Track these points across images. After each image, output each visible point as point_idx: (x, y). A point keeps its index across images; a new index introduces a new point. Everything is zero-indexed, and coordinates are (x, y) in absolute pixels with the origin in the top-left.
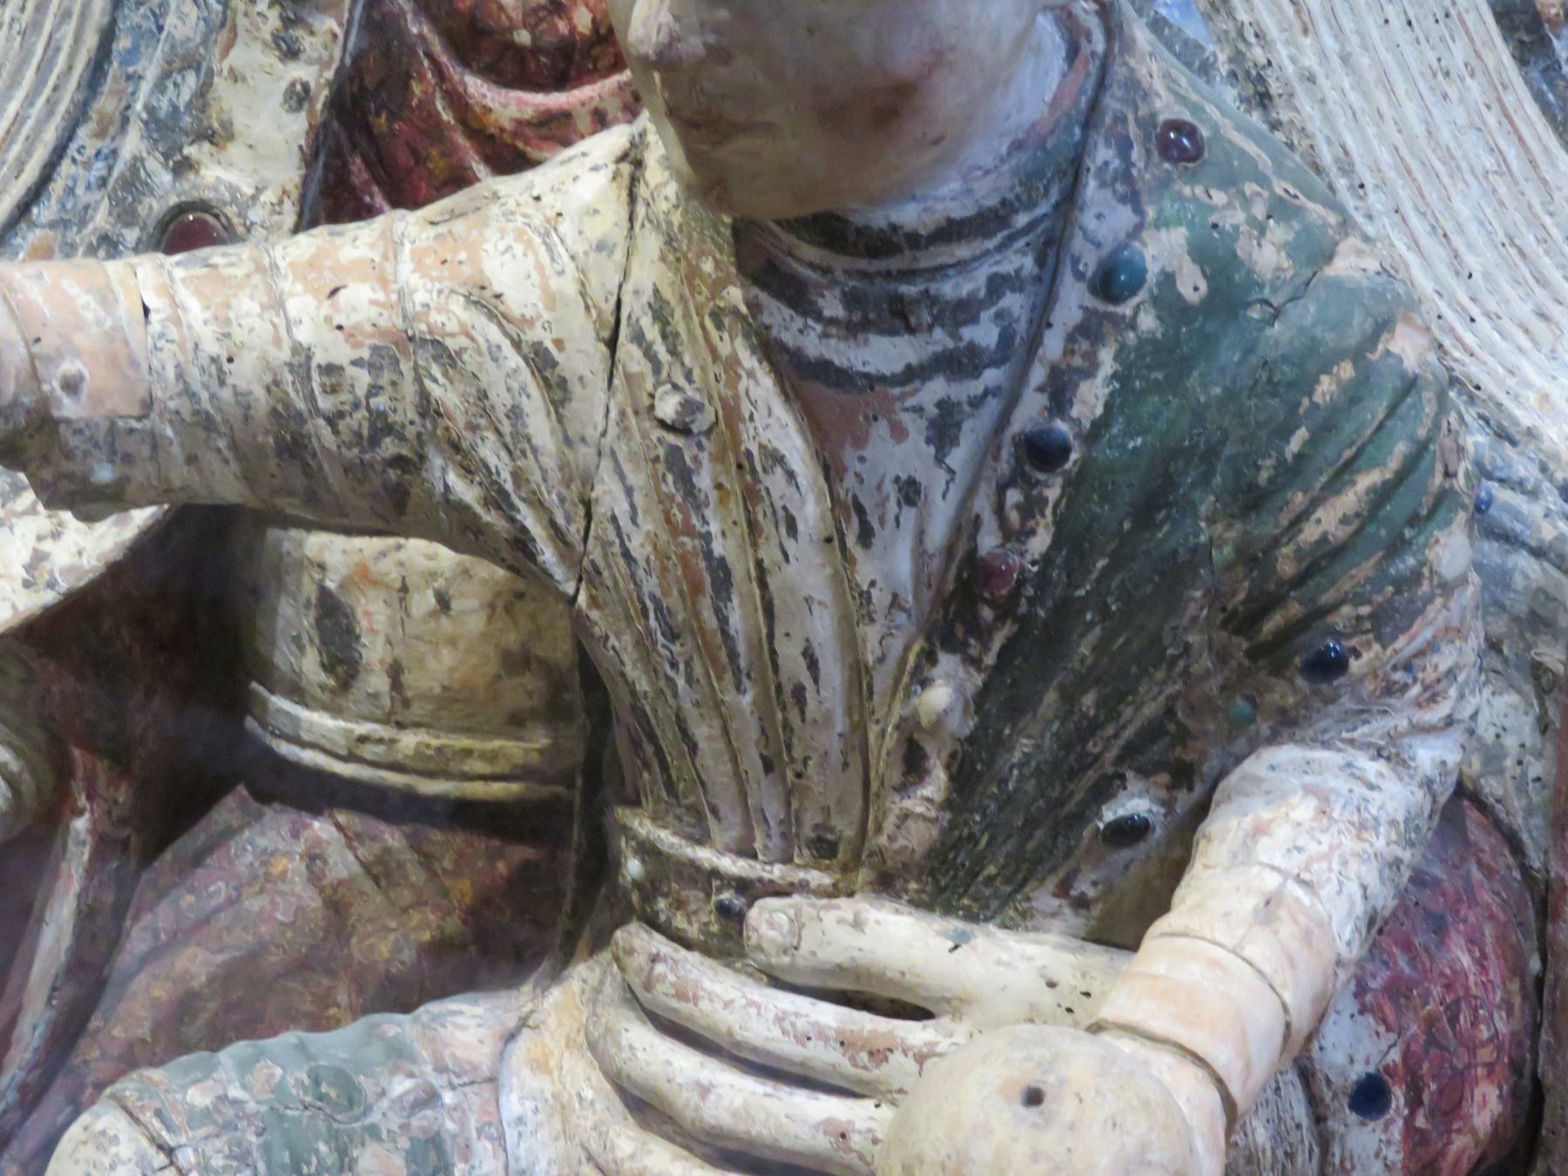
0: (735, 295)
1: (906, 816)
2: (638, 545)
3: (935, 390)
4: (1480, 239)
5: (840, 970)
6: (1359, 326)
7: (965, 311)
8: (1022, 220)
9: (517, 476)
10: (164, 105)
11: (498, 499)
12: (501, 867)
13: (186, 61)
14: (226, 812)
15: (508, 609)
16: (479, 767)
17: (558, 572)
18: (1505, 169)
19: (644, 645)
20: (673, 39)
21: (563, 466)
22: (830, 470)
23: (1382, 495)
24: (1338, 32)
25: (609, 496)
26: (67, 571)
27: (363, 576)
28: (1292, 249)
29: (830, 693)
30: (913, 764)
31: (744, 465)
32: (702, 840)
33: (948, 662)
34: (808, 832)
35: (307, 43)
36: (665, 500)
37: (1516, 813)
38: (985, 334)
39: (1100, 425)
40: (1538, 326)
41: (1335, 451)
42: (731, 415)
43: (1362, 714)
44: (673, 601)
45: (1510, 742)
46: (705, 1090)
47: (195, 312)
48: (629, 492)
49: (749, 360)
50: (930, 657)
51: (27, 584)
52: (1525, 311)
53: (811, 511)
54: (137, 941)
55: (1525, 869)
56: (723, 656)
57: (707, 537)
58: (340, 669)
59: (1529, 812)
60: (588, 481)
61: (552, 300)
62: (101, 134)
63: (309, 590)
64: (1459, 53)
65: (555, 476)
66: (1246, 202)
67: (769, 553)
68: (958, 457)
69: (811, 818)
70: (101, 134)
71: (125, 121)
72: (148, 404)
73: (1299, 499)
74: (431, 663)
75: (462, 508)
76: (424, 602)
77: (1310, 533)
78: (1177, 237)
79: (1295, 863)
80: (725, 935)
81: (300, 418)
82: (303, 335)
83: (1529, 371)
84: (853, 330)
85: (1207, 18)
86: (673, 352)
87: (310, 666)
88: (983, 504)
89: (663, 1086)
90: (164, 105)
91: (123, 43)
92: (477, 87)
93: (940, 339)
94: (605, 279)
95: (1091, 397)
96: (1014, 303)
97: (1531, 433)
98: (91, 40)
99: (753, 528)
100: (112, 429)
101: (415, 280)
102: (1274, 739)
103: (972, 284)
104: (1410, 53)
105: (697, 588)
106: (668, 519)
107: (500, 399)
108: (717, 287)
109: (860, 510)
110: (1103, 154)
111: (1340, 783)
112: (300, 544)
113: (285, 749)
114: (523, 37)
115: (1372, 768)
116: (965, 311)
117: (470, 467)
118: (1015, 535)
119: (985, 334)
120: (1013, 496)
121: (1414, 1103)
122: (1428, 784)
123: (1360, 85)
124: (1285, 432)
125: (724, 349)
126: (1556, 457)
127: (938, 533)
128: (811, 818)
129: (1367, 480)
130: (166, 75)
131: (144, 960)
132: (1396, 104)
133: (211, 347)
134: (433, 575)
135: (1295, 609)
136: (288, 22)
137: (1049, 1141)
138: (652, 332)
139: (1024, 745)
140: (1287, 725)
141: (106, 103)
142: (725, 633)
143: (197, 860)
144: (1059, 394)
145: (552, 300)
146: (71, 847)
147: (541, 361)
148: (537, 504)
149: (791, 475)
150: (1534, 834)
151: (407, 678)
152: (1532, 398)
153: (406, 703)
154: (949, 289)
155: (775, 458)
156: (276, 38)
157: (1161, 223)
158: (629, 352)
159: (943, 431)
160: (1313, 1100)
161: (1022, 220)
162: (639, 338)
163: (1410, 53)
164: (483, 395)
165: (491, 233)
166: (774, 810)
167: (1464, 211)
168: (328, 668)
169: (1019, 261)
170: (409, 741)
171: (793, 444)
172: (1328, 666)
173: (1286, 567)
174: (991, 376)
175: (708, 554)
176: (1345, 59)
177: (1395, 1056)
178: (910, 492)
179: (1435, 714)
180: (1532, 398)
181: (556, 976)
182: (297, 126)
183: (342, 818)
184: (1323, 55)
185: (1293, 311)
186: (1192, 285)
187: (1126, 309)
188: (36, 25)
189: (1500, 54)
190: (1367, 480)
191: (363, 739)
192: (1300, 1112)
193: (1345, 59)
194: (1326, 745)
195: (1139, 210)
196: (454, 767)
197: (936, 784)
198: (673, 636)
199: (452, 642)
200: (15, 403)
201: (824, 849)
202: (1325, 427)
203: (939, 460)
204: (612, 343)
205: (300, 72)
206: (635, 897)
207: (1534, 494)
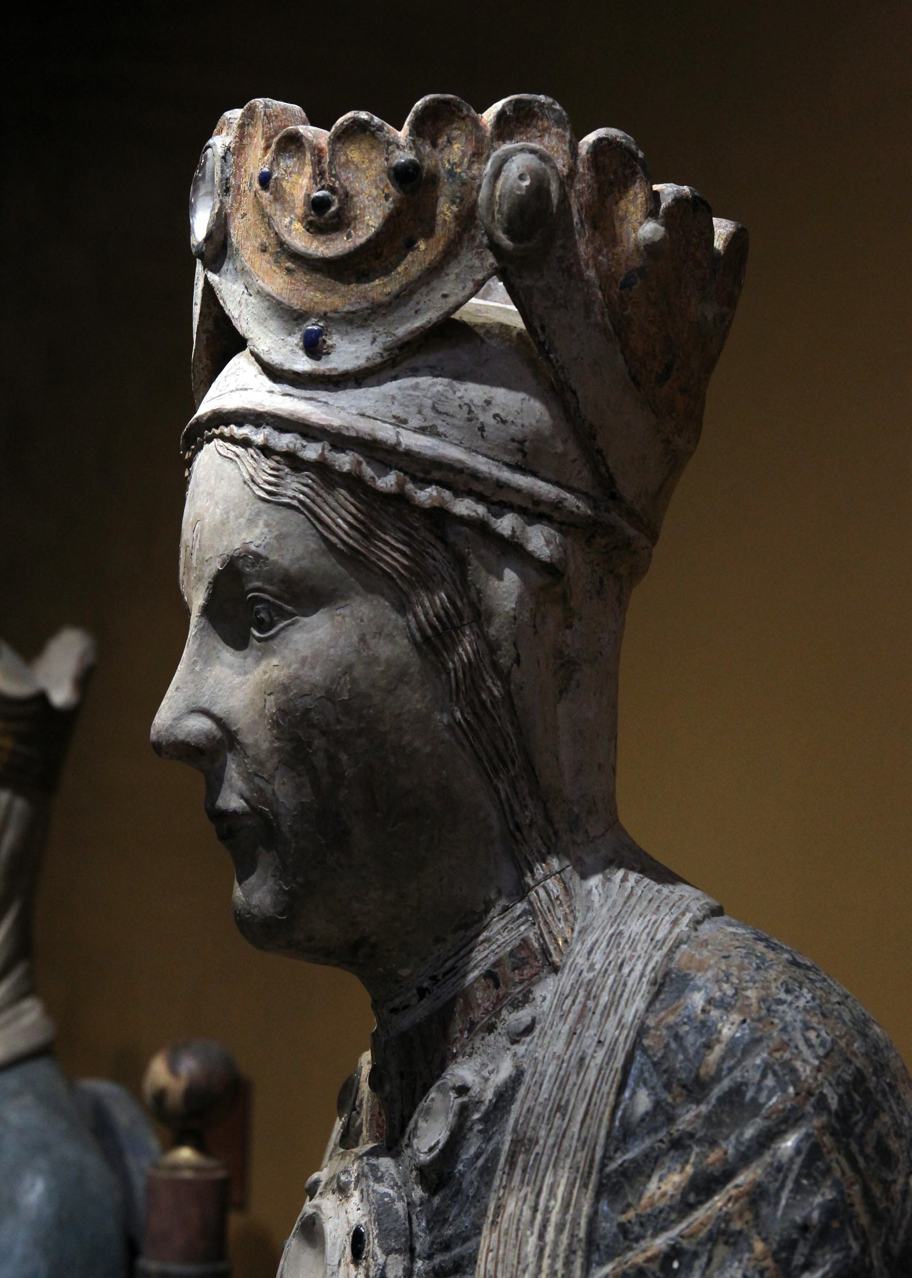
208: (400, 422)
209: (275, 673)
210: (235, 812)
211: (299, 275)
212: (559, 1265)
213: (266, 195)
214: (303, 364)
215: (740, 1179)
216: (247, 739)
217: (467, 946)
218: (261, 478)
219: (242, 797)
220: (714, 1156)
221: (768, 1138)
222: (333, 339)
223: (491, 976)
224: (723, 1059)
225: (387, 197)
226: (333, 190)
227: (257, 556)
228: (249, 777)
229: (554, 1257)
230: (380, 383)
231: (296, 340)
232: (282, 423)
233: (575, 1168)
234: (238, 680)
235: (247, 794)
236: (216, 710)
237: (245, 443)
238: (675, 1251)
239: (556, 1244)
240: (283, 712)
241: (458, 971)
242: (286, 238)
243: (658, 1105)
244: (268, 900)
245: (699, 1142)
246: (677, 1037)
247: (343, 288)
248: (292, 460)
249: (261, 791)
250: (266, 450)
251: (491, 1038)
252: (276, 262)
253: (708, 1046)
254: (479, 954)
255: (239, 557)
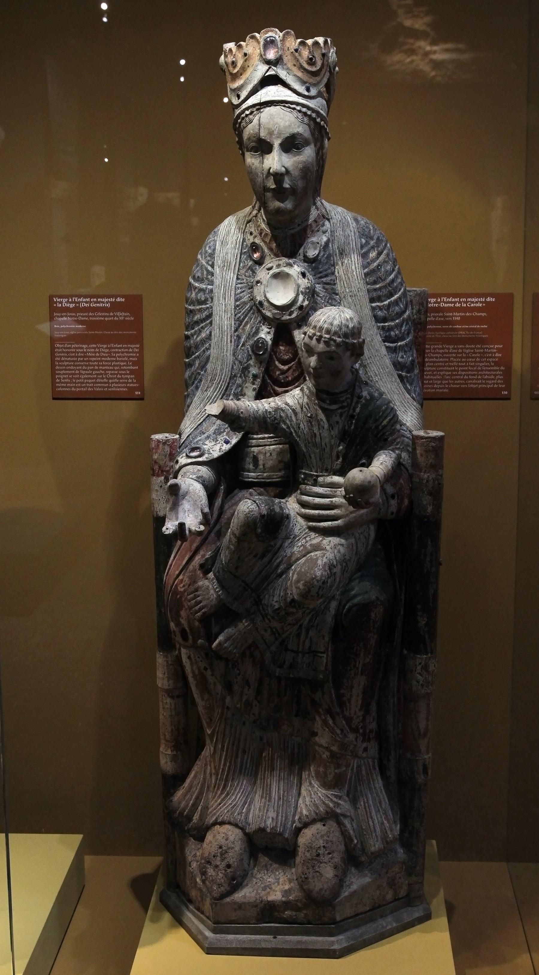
0: (316, 401)
1: (337, 464)
2: (305, 432)
3: (340, 411)
4: (398, 402)
5: (330, 483)
6: (386, 402)
7: (343, 402)
8: (349, 391)
9: (291, 424)
10: (236, 392)
11: (288, 427)
12: (277, 491)
13: (239, 386)
14: (236, 491)
15: (279, 455)
16: (275, 477)
17: (295, 437)
18: (400, 394)
19: (305, 445)
20: (316, 366)
21: (296, 423)
22: (328, 420)
23: (390, 420)
24: (380, 377)
25: (302, 425)
26: (224, 450)
27: (260, 452)
28: (379, 394)
29: (328, 449)
30: (338, 458)
31: (318, 421)
32: (312, 471)
33: (342, 443)
34: (325, 468)
35: (256, 383)
36: (308, 426)
37: (407, 466)
38: (345, 404)
39: (359, 413)
40: (405, 412)
41: (385, 415)
42: (317, 415)
43: (390, 446)
44: (309, 439)
45: (406, 458)
46: (314, 500)
47: (254, 406)
48: (304, 425)
49: (318, 409)
50: (340, 443)
51: (219, 452)
52: (403, 410)
53: (326, 426)
54: (226, 507)
55: (409, 473)
56: (315, 445)
57: (313, 430)
58: (256, 466)
59: (409, 466)
60: (299, 424)
61: (295, 404)
62: (226, 397)
63: (251, 455)
64: (394, 380)
65: (295, 424)
66: (373, 389)
67: (321, 431)
68: (343, 418)
69: (325, 466)
70: (226, 397)
71: (230, 395)
72: (250, 415)
73: (381, 420)
74: (269, 463)
75: (284, 429)
76: (268, 454)
77: (383, 424)
78: (366, 392)
79: (384, 460)
80: (314, 483)
81: (266, 418)
82: (266, 408)
83: (405, 417)
84: (330, 404)
85: (365, 375)
86: (309, 409)
87: (251, 467)
88: (346, 423)
89: (308, 501)
90: (236, 392)
91: (231, 385)
92: (277, 388)
93: (340, 405)
94: (301, 401)
95: (358, 410)
96: (349, 400)
97: (405, 424)
98: (227, 384)
99: (319, 428)
100: (246, 418)
101: (278, 402)
102: (380, 450)
103: (344, 398)
104: (388, 379)
105: (312, 436)
106: (309, 429)
107: (289, 415)
108: (314, 401)
109: (332, 425)
110: (357, 384)
111: (387, 454)
112: (250, 450)
113: (246, 480)
114: (283, 381)
115: (391, 452)
116: (343, 402)
117: (285, 423)
118: (350, 427)
119: (345, 404)
120: (349, 422)
121: (398, 498)
122: (397, 455)
123: (383, 383)
124: (380, 413)
125: (315, 408)
126: (408, 427)
127: (341, 426)
128: (325, 466)
129: (389, 418)
130: (237, 388)
131: (228, 508)
132: (387, 385)
133: (256, 409)
134: (270, 451)
135: (381, 433)
136: (254, 380)
137: (364, 474)
138: (307, 407)
139: (351, 454)
140: (382, 448)
141: (228, 392)
142: (316, 443)
143: (233, 497)
144: (354, 410)
145: (295, 404)
146: (220, 491)
147: (294, 410)
148: (293, 428)
149: (324, 422)
150: (409, 468)
151: (266, 466)
152: (405, 420)
153: (265, 469)
154: (341, 399)
155: (322, 420)
156: (252, 382)
157: (364, 391)
158: (304, 409)
159: (341, 415)
160: (386, 497)
161: (349, 391)
162: (305, 407)
163: (388, 379)
164: (287, 415)
165: (287, 397)
166: (321, 466)
167: (395, 398)
168: (254, 466)
169: (349, 396)
170: (265, 474)
171: (324, 419)
172: (386, 440)
173: (380, 428)
174: (346, 409)
175: (314, 432)
176: (381, 379)
177: (395, 491)
178: (337, 423)
179: (398, 446)
180: (405, 420)
181: (290, 496)
182: (254, 393)
183: (254, 488)
184: (378, 379)
185: (379, 400)
186: (368, 397)
187: (361, 400)
188: (219, 383)
189: (398, 380)
190: (389, 418)
191: (259, 475)
192: (385, 498)
193: (381, 379)
194: (386, 450)
195: (362, 390)
196: (271, 477)
197: (340, 460)
198: (309, 443)
199: (272, 460)
200: (236, 415)
201: (327, 470)
202: (384, 412)
203: (341, 419)
204: (302, 408)
205: (255, 386)
206: (302, 482)
207: (406, 431)
208: (319, 107)
209: (302, 159)
210: (288, 188)
211: (305, 73)
212: (360, 270)
213: (297, 54)
214: (306, 93)
215: (385, 252)
216: (292, 172)
217: (308, 216)
218: (300, 117)
219: (289, 185)
220: (379, 249)
221: (386, 245)
222: (311, 88)
223: (315, 221)
224: (373, 232)
225: (321, 59)
226: (313, 56)
227: (301, 134)
228: (291, 181)
229: (358, 269)
230: (316, 99)
231: (304, 87)
232: (303, 106)
233: (357, 253)
234: (288, 160)
235: (291, 184)
236: (285, 166)
237: (294, 109)
238: (379, 265)
239: (358, 267)
240: (304, 167)
241: (307, 220)
242: (303, 64)
243: (366, 241)
244: (291, 206)
245: (376, 247)
246: (363, 229)
247: (313, 78)
248: (305, 114)
249: (294, 183)
250: (300, 111)
251: (318, 233)
252: (299, 69)
253: (370, 230)
254: (311, 217)
255: (296, 134)
